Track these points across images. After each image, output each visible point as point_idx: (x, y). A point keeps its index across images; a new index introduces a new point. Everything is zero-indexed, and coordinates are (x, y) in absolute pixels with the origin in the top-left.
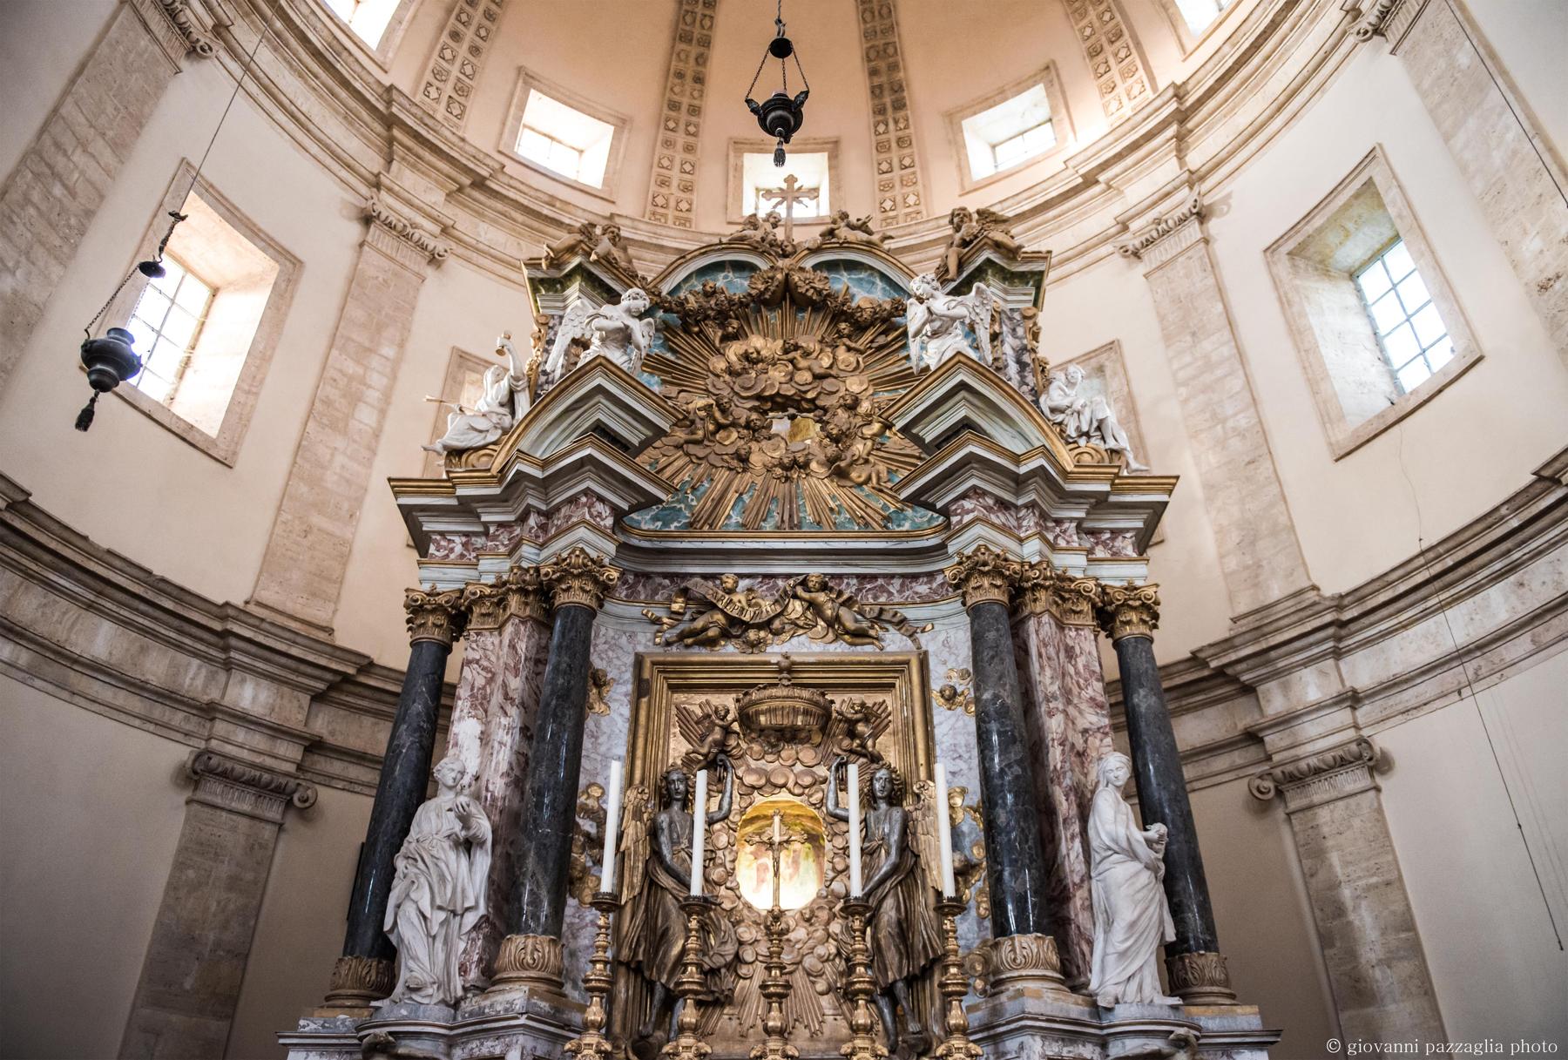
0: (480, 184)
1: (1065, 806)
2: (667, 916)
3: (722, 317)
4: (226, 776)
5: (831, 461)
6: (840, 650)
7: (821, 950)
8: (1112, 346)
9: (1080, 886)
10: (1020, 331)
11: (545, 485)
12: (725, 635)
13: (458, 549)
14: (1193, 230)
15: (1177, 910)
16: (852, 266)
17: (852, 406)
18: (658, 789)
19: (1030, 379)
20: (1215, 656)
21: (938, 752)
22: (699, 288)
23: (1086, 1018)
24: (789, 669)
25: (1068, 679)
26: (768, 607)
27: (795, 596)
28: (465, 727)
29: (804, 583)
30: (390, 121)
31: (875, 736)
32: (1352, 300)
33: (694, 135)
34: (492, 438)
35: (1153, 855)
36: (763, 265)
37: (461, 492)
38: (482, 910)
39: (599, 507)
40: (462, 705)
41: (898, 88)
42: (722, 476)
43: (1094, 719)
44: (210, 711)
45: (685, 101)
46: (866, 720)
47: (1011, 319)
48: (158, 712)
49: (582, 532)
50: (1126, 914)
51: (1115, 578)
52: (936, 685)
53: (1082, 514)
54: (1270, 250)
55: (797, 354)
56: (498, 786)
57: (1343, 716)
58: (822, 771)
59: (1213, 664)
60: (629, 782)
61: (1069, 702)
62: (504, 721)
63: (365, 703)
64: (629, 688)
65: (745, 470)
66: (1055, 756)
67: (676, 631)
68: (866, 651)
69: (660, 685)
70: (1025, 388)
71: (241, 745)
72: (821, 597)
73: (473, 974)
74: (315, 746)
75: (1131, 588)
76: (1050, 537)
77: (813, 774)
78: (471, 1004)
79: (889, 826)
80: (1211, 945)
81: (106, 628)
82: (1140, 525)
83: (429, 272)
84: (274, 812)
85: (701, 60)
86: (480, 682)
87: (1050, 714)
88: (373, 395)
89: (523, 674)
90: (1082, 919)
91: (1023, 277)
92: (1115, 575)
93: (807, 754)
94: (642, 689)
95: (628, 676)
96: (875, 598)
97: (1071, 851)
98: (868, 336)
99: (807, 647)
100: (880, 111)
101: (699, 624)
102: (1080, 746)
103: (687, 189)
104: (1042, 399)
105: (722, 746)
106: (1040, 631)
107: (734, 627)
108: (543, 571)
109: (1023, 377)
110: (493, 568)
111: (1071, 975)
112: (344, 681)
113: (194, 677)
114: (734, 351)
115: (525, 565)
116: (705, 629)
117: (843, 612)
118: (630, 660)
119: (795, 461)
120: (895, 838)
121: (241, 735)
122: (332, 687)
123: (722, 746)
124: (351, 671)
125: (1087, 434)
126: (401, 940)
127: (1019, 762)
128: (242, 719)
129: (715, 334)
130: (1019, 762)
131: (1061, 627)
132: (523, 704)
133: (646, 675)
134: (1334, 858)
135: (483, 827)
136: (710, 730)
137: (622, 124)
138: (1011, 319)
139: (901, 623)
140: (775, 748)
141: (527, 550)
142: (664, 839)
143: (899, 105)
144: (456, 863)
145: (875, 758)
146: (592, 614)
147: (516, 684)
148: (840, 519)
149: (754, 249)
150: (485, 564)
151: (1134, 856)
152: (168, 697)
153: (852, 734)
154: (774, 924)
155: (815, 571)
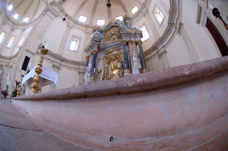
4: (81, 73)
8: (144, 23)
11: (92, 46)
12: (109, 53)
14: (147, 13)
24: (114, 55)
28: (89, 65)
35: (137, 61)
44: (79, 69)
48: (76, 69)
57: (163, 48)
68: (120, 51)
69: (104, 58)
72: (116, 48)
81: (72, 65)
82: (139, 35)
91: (129, 19)
92: (137, 40)
93: (116, 61)
94: (103, 59)
99: (115, 52)
100: (125, 12)
113: (78, 67)
114: (109, 32)
121: (81, 70)
123: (109, 62)
128: (81, 69)
129: (108, 31)
131: (132, 45)
143: (126, 11)
144: (88, 74)
151: (136, 62)
152: (76, 68)
155: (115, 47)
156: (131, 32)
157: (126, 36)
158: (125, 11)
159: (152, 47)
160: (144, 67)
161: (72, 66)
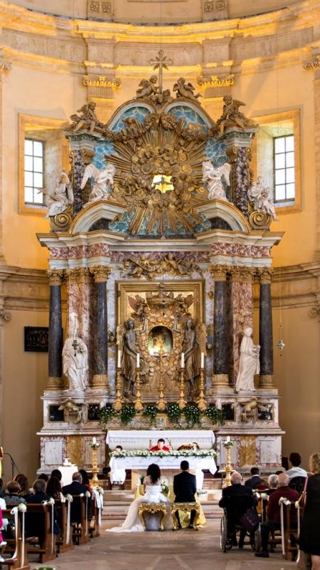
2: (131, 362)
5: (176, 206)
7: (172, 369)
9: (236, 360)
10: (244, 158)
12: (143, 274)
13: (59, 253)
15: (262, 364)
16: (185, 108)
18: (125, 326)
19: (245, 181)
20: (305, 267)
21: (206, 313)
23: (232, 394)
25: (242, 301)
27: (164, 260)
28: (73, 315)
29: (167, 257)
31: (188, 307)
34: (63, 210)
35: (255, 354)
36: (151, 110)
37: (61, 239)
38: (88, 367)
39: (105, 246)
40: (71, 309)
42: (138, 209)
43: (248, 312)
46: (186, 303)
47: (241, 152)
49: (102, 258)
50: (245, 370)
51: (262, 264)
52: (207, 291)
53: (252, 244)
55: (164, 155)
56: (86, 334)
58: (172, 317)
59: (305, 269)
60: (116, 324)
61: (241, 308)
62: (85, 315)
63: (18, 280)
64: (114, 292)
65: (146, 208)
66: (235, 325)
67: (127, 272)
70: (243, 186)
73: (87, 382)
75: (265, 268)
76: (242, 251)
77: (169, 318)
78: (89, 390)
80: (271, 372)
86: (75, 301)
87: (235, 313)
89: (88, 300)
90: (235, 368)
91: (249, 134)
93: (168, 312)
94: (118, 294)
95: (113, 288)
96: (190, 260)
97: (235, 351)
101: (134, 272)
102: (242, 320)
104: (248, 191)
105: (143, 311)
106: (235, 286)
107: (145, 272)
108: (91, 270)
109: (243, 180)
110: (72, 264)
111: (231, 383)
115: (84, 266)
116: (137, 273)
117: (179, 267)
118: (114, 282)
119: (164, 205)
120: (192, 341)
122: (9, 277)
123: (143, 311)
124: (14, 273)
125: (261, 208)
126: (68, 374)
127: (223, 330)
130: (223, 330)
132: (89, 310)
133: (119, 289)
135: (86, 348)
136: (139, 306)
138: (241, 152)
139: (198, 269)
140: (157, 311)
141: (84, 260)
142: (129, 342)
144: (79, 356)
146: (105, 283)
147: (86, 304)
148: (179, 227)
149: (146, 102)
150: (70, 261)
151: (250, 355)
153: (181, 306)
154: (158, 359)
159: (299, 266)
160: (267, 368)
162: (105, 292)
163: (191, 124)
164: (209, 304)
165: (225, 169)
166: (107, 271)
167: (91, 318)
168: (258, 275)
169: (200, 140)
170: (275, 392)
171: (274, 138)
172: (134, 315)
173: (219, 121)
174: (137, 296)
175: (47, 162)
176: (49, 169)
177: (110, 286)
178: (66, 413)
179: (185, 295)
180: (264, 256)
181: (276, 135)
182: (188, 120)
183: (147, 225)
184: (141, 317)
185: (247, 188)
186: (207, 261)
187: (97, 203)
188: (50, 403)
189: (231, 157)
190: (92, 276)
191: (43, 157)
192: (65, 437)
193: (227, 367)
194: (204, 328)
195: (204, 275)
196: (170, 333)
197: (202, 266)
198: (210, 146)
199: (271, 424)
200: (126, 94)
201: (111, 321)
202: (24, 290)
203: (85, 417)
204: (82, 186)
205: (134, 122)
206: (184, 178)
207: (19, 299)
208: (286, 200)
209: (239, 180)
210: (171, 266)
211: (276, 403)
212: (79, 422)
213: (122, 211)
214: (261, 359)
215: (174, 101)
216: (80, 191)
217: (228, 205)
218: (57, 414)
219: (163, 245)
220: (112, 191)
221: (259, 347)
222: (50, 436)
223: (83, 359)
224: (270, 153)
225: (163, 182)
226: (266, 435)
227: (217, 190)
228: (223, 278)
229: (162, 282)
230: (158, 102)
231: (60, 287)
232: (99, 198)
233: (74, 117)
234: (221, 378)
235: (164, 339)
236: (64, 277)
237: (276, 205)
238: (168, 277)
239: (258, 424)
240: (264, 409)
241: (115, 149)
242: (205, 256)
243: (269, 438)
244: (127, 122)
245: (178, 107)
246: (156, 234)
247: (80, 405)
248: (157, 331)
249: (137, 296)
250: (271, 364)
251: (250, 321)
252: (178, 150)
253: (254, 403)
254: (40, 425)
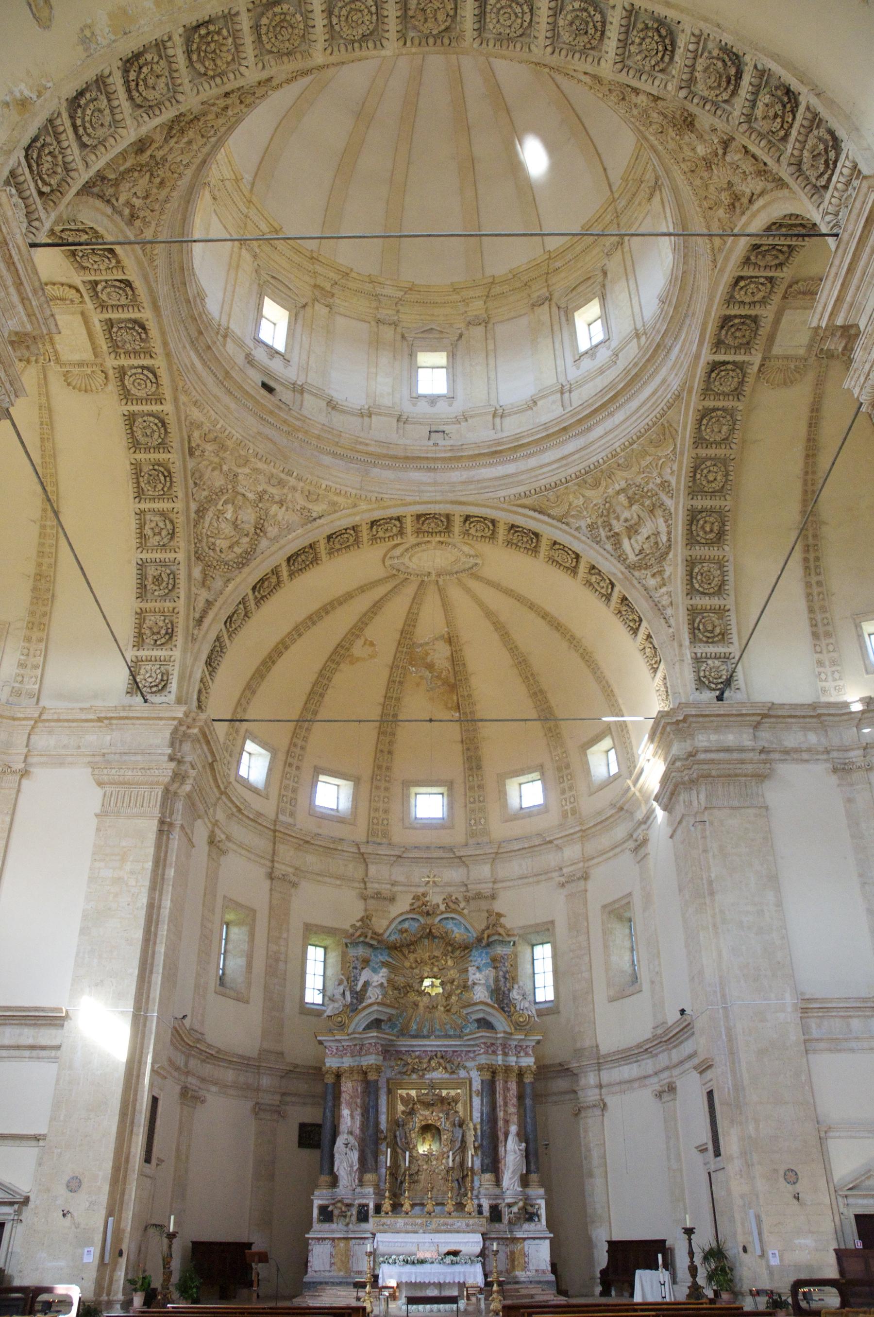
0: (307, 842)
1: (501, 1137)
3: (408, 946)
4: (265, 1110)
6: (447, 1076)
8: (552, 922)
14: (582, 882)
16: (453, 919)
17: (452, 982)
22: (399, 927)
26: (425, 1066)
28: (345, 1112)
30: (275, 831)
32: (627, 931)
33: (389, 782)
37: (337, 1037)
40: (343, 1106)
41: (479, 759)
44: (258, 1090)
45: (385, 765)
49: (374, 1056)
52: (474, 1089)
54: (604, 907)
56: (358, 1132)
66: (501, 1123)
71: (267, 1099)
74: (284, 1094)
78: (358, 1190)
79: (458, 1133)
81: (231, 1072)
83: (293, 890)
84: (275, 1117)
85: (391, 743)
88: (282, 957)
94: (389, 1092)
97: (501, 1150)
98: (458, 952)
99: (438, 1075)
103: (386, 811)
105: (413, 1109)
106: (499, 1086)
107: (414, 1071)
110: (347, 1062)
111: (498, 1182)
112: (292, 1072)
114: (412, 957)
123: (413, 1109)
134: (590, 1134)
137: (357, 781)
139: (465, 1067)
143: (479, 767)
145: (456, 1112)
147: (359, 1101)
148: (448, 1027)
149: (419, 913)
150: (345, 1059)
154: (428, 1157)
156: (511, 1034)
157: (493, 1044)
158: (474, 765)
159: (560, 1065)
161: (229, 1075)
162: (377, 1090)
163: (458, 934)
164: (477, 1101)
165: (490, 972)
166: (379, 1069)
167: (363, 1115)
168: (521, 1074)
169: (466, 947)
170: (541, 1191)
171: (533, 946)
172: (403, 1112)
173: (483, 931)
174: (408, 1094)
175: (328, 966)
176: (329, 972)
177: (382, 1084)
178: (336, 1212)
179: (453, 1093)
180: (527, 1054)
181: (534, 942)
182: (456, 930)
183: (418, 1024)
184: (411, 1113)
185: (509, 990)
186: (473, 1059)
187: (371, 1005)
188: (321, 1202)
189: (495, 962)
190: (365, 1073)
191: (325, 962)
192: (333, 1239)
193: (493, 1166)
194: (471, 1125)
195: (471, 1073)
196: (438, 1130)
197: (469, 1064)
198: (475, 953)
199: (539, 1227)
200: (402, 905)
201: (383, 1118)
202: (302, 1087)
203: (354, 1218)
204: (359, 988)
205: (406, 931)
206: (452, 982)
207: (295, 1095)
208: (546, 1002)
209: (501, 984)
210: (440, 1064)
211: (542, 1203)
212: (347, 1225)
213: (394, 1012)
214: (527, 1157)
215: (442, 913)
216: (357, 993)
217: (493, 1007)
218: (326, 1215)
219: (433, 1044)
220: (385, 995)
221: (524, 1145)
222: (318, 1239)
223: (355, 1156)
224: (530, 959)
225: (433, 985)
226: (534, 1238)
227: (480, 994)
228: (487, 1076)
229: (431, 1080)
230: (428, 914)
231: (334, 1084)
232: (373, 1000)
233: (353, 926)
234: (488, 1176)
235: (433, 1137)
236: (338, 1076)
237: (537, 1007)
238: (438, 1075)
239: (526, 1226)
240: (530, 1209)
241: (389, 955)
242: (472, 1055)
243: (537, 1241)
244: (402, 932)
245: (447, 918)
246: (425, 1032)
247: (349, 1206)
248: (426, 1129)
249: (408, 1094)
250: (537, 1162)
251: (515, 1118)
252: (446, 955)
253: (521, 1204)
254: (309, 1227)
